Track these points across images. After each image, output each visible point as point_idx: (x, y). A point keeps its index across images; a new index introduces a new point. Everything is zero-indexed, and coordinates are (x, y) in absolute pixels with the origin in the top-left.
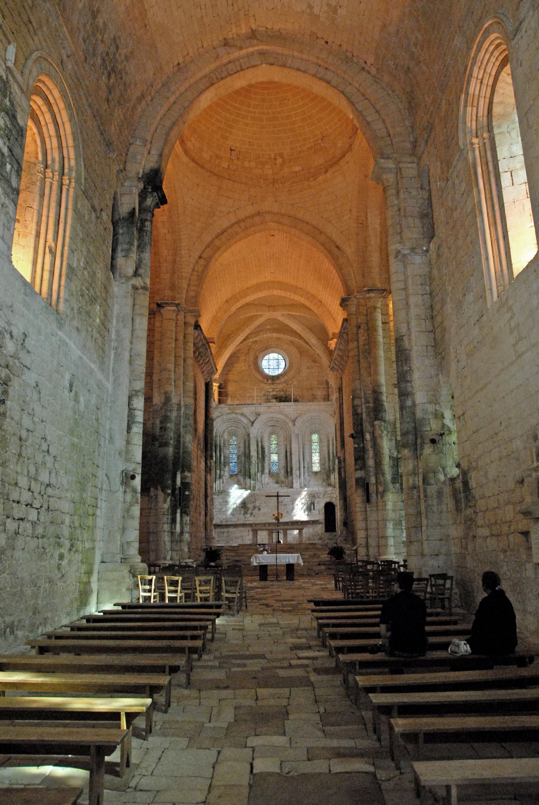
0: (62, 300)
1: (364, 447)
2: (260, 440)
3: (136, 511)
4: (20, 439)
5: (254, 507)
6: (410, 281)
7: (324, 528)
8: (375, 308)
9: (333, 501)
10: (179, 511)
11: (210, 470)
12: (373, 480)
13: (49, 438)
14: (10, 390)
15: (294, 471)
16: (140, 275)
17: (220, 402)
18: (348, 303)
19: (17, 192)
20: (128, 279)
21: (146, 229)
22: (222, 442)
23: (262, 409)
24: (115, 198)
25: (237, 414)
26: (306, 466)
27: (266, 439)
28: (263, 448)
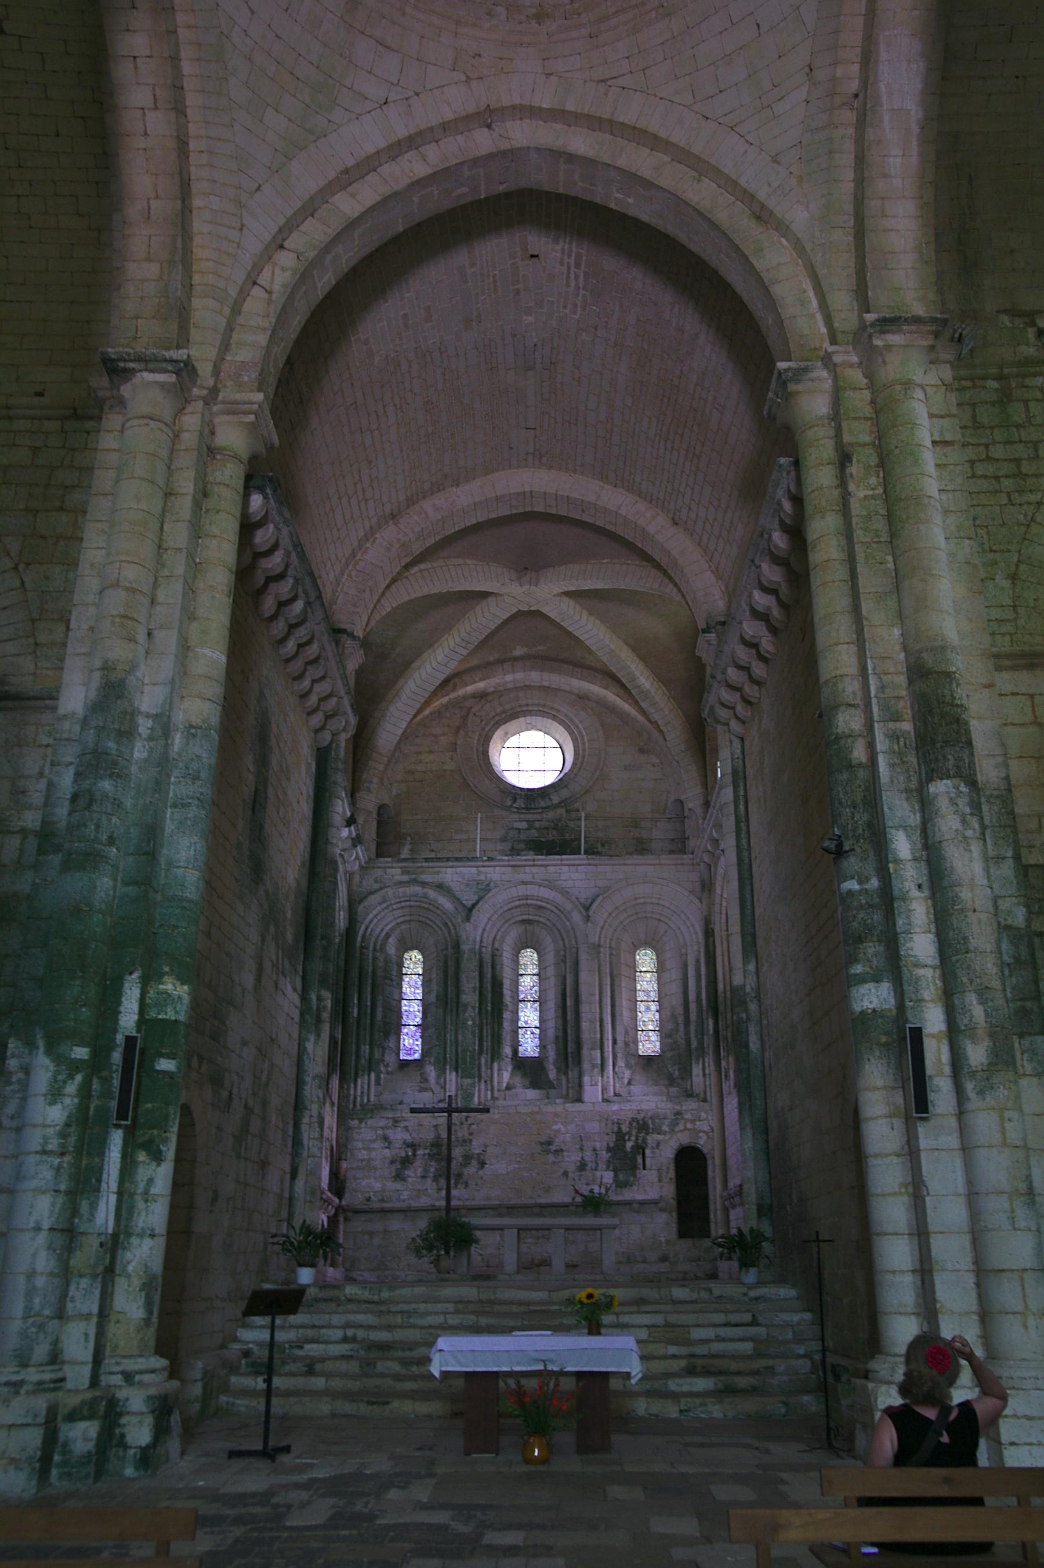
2: (487, 958)
5: (467, 1158)
7: (674, 1227)
9: (702, 1142)
10: (117, 1139)
12: (933, 1020)
15: (585, 1052)
18: (799, 387)
23: (494, 873)
25: (424, 884)
26: (620, 1038)
28: (497, 985)
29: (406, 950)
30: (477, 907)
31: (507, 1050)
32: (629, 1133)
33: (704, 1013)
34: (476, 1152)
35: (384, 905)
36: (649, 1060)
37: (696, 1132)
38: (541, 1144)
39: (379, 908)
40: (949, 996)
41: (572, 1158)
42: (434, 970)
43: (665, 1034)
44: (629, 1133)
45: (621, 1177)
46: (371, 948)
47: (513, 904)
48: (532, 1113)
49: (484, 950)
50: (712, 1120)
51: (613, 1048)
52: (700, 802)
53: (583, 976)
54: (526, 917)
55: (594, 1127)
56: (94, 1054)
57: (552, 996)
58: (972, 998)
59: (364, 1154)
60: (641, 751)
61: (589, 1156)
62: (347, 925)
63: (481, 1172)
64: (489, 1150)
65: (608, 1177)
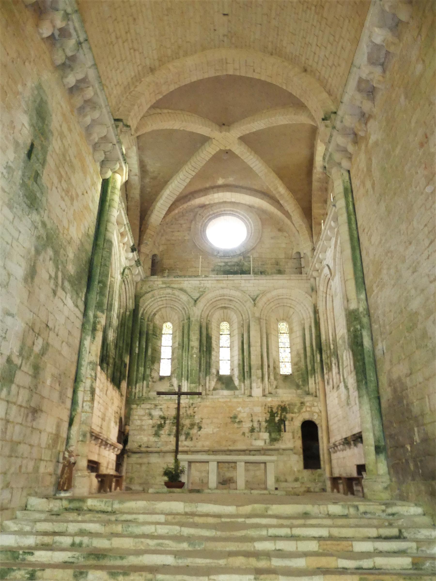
2: (204, 325)
5: (192, 425)
9: (315, 418)
22: (151, 328)
27: (213, 325)
28: (209, 338)
29: (165, 322)
30: (199, 299)
31: (214, 371)
32: (277, 413)
33: (315, 352)
34: (197, 422)
35: (152, 299)
36: (286, 377)
37: (313, 413)
38: (231, 418)
39: (150, 300)
41: (247, 425)
42: (178, 331)
43: (295, 364)
44: (277, 413)
45: (273, 435)
46: (146, 320)
47: (217, 299)
48: (226, 402)
49: (202, 320)
51: (268, 369)
52: (310, 249)
53: (252, 333)
54: (223, 305)
55: (258, 410)
59: (138, 423)
60: (280, 230)
61: (256, 425)
62: (134, 307)
63: (199, 433)
64: (204, 421)
65: (266, 436)
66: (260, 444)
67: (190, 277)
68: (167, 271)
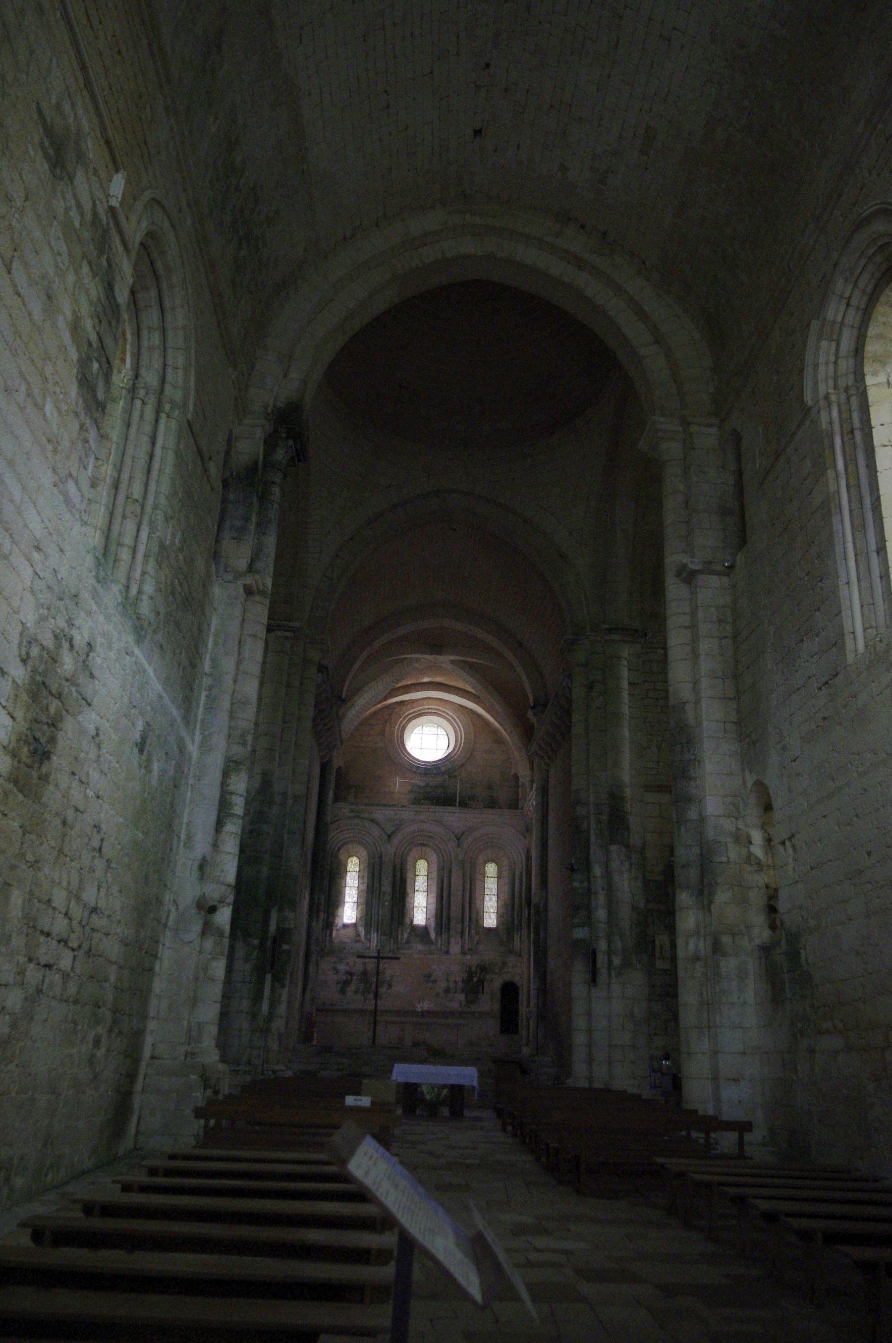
0: (144, 597)
1: (589, 890)
2: (399, 866)
3: (219, 968)
4: (64, 823)
6: (700, 614)
8: (619, 658)
9: (517, 979)
10: (269, 977)
11: (318, 911)
12: (603, 945)
13: (104, 827)
14: (60, 736)
16: (258, 572)
17: (336, 799)
19: (101, 407)
20: (238, 576)
21: (272, 497)
23: (406, 815)
24: (229, 440)
28: (403, 881)
40: (609, 937)
43: (500, 916)
50: (521, 971)
56: (261, 943)
57: (434, 889)
58: (617, 938)
61: (451, 985)
65: (462, 997)
66: (454, 1006)
67: (385, 805)
68: (353, 790)
